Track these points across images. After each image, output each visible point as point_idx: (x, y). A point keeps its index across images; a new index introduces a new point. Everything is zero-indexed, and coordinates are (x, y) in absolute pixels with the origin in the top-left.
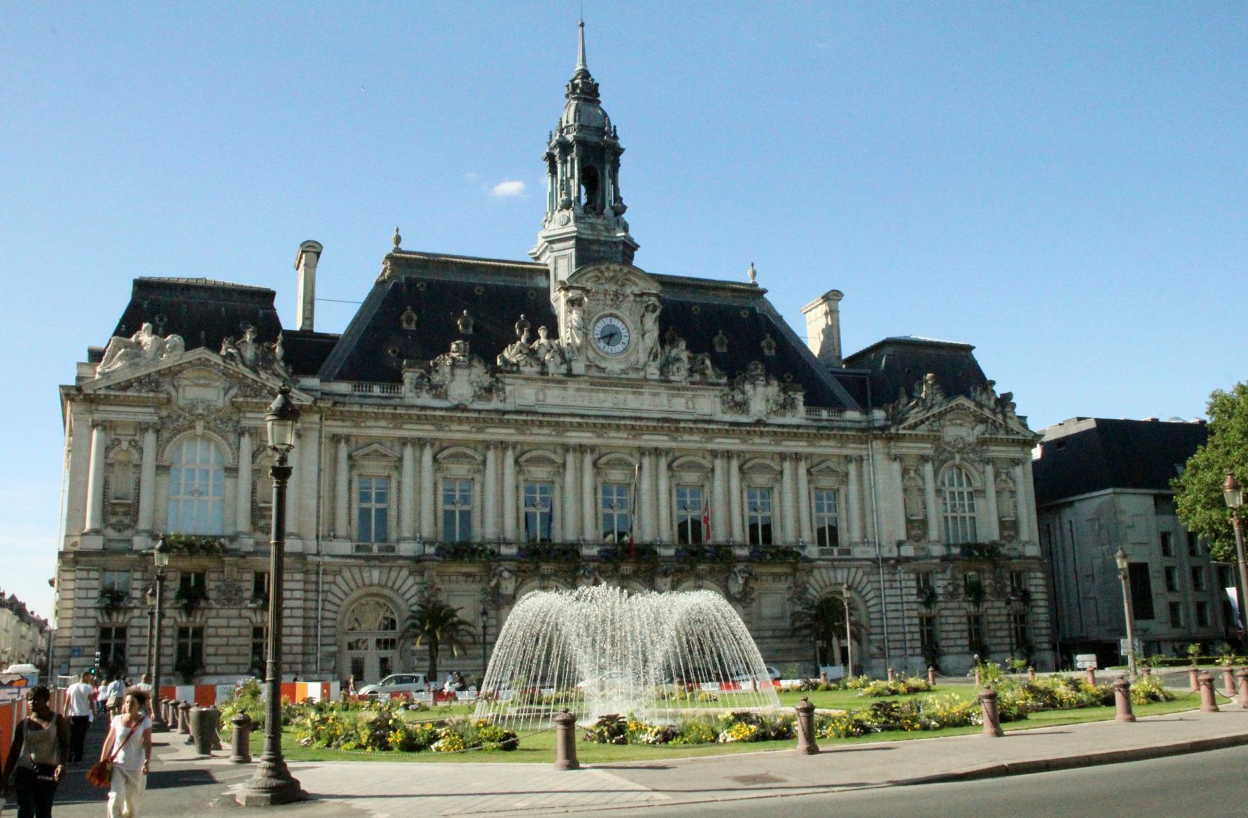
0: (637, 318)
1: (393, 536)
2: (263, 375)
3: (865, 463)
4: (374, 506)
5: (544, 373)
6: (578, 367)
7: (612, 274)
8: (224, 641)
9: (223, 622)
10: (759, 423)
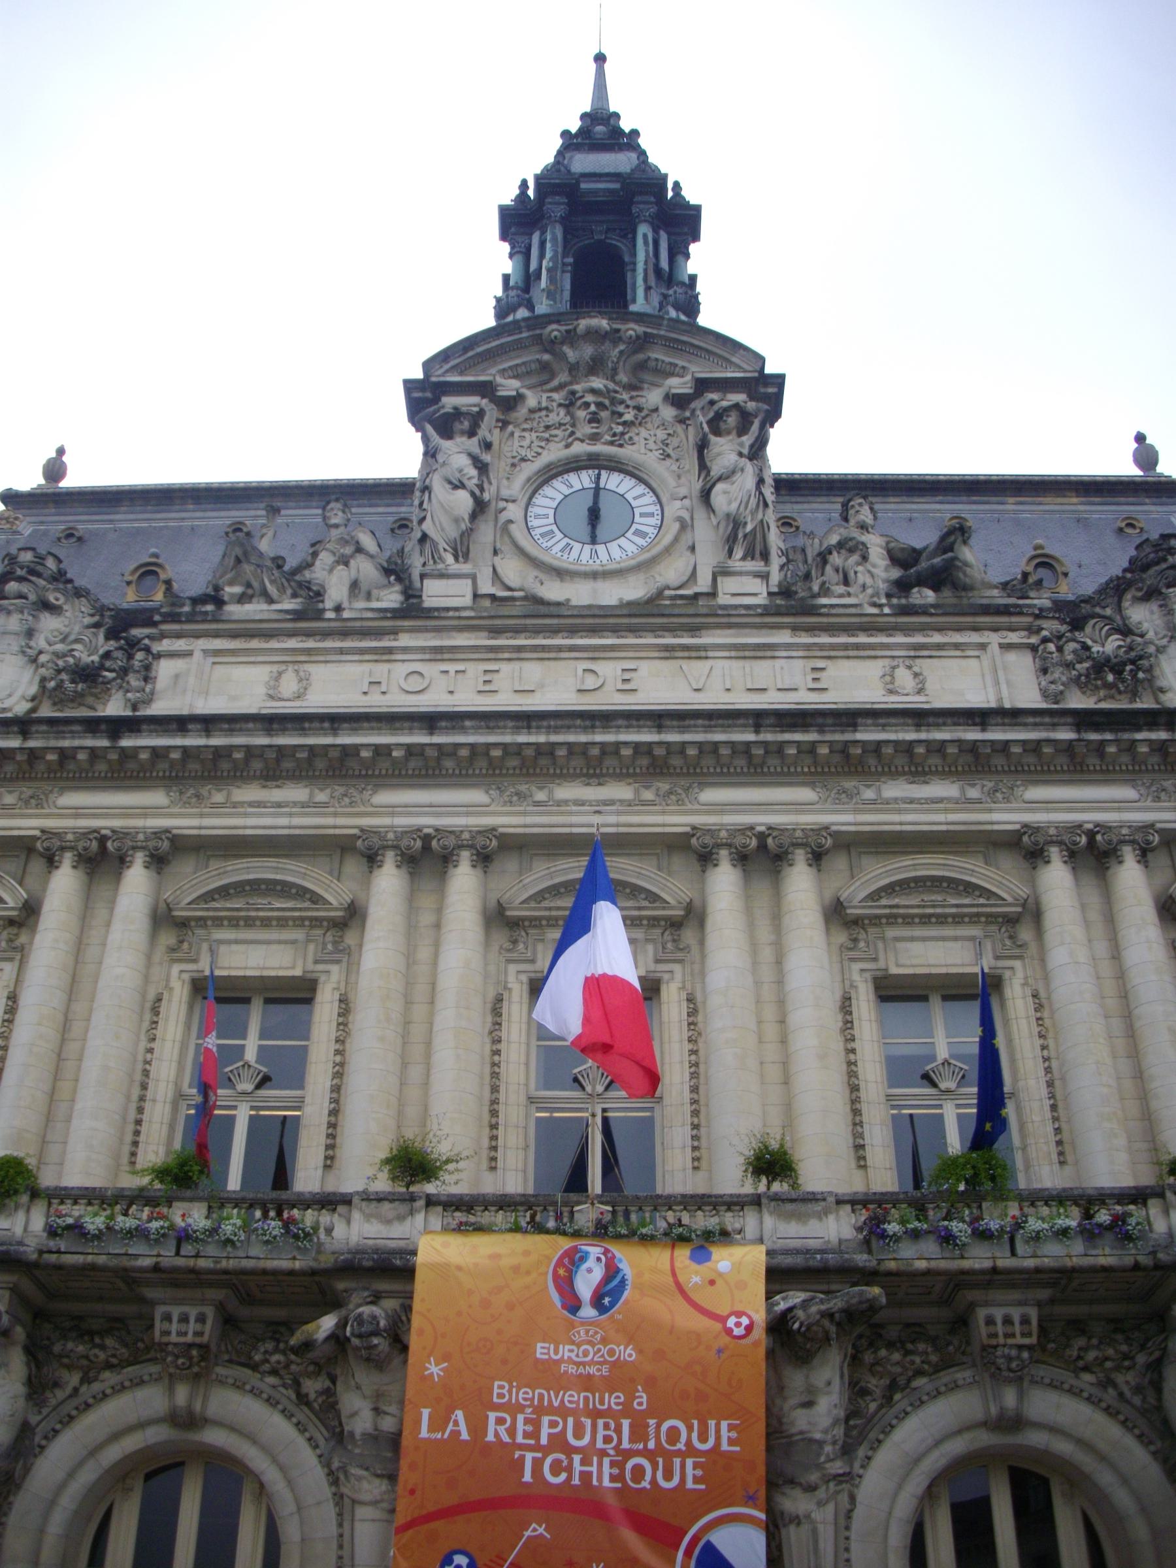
0: (690, 462)
7: (588, 351)
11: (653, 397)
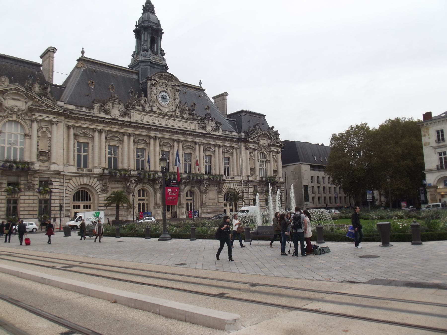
1: (90, 166)
2: (43, 98)
3: (238, 149)
4: (82, 153)
5: (144, 110)
6: (155, 109)
8: (27, 205)
9: (27, 198)
10: (209, 134)
11: (170, 83)
